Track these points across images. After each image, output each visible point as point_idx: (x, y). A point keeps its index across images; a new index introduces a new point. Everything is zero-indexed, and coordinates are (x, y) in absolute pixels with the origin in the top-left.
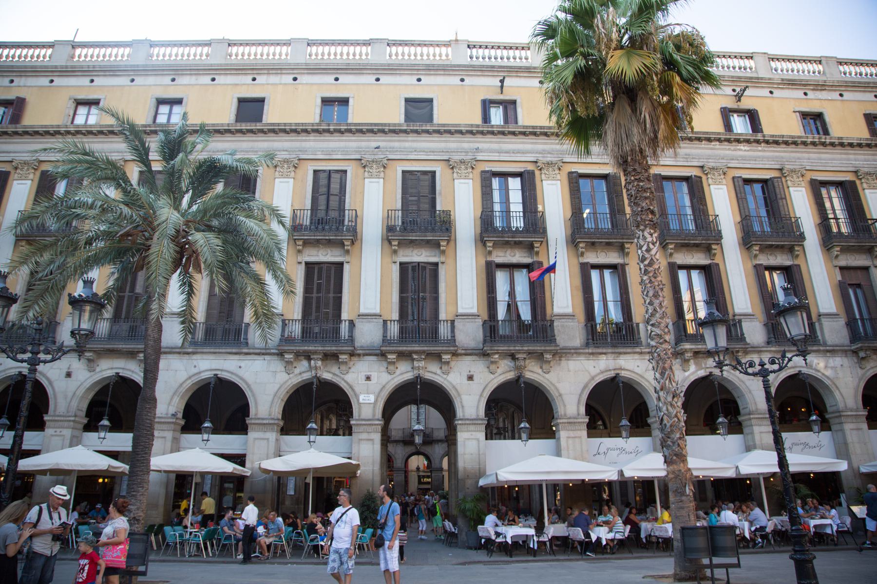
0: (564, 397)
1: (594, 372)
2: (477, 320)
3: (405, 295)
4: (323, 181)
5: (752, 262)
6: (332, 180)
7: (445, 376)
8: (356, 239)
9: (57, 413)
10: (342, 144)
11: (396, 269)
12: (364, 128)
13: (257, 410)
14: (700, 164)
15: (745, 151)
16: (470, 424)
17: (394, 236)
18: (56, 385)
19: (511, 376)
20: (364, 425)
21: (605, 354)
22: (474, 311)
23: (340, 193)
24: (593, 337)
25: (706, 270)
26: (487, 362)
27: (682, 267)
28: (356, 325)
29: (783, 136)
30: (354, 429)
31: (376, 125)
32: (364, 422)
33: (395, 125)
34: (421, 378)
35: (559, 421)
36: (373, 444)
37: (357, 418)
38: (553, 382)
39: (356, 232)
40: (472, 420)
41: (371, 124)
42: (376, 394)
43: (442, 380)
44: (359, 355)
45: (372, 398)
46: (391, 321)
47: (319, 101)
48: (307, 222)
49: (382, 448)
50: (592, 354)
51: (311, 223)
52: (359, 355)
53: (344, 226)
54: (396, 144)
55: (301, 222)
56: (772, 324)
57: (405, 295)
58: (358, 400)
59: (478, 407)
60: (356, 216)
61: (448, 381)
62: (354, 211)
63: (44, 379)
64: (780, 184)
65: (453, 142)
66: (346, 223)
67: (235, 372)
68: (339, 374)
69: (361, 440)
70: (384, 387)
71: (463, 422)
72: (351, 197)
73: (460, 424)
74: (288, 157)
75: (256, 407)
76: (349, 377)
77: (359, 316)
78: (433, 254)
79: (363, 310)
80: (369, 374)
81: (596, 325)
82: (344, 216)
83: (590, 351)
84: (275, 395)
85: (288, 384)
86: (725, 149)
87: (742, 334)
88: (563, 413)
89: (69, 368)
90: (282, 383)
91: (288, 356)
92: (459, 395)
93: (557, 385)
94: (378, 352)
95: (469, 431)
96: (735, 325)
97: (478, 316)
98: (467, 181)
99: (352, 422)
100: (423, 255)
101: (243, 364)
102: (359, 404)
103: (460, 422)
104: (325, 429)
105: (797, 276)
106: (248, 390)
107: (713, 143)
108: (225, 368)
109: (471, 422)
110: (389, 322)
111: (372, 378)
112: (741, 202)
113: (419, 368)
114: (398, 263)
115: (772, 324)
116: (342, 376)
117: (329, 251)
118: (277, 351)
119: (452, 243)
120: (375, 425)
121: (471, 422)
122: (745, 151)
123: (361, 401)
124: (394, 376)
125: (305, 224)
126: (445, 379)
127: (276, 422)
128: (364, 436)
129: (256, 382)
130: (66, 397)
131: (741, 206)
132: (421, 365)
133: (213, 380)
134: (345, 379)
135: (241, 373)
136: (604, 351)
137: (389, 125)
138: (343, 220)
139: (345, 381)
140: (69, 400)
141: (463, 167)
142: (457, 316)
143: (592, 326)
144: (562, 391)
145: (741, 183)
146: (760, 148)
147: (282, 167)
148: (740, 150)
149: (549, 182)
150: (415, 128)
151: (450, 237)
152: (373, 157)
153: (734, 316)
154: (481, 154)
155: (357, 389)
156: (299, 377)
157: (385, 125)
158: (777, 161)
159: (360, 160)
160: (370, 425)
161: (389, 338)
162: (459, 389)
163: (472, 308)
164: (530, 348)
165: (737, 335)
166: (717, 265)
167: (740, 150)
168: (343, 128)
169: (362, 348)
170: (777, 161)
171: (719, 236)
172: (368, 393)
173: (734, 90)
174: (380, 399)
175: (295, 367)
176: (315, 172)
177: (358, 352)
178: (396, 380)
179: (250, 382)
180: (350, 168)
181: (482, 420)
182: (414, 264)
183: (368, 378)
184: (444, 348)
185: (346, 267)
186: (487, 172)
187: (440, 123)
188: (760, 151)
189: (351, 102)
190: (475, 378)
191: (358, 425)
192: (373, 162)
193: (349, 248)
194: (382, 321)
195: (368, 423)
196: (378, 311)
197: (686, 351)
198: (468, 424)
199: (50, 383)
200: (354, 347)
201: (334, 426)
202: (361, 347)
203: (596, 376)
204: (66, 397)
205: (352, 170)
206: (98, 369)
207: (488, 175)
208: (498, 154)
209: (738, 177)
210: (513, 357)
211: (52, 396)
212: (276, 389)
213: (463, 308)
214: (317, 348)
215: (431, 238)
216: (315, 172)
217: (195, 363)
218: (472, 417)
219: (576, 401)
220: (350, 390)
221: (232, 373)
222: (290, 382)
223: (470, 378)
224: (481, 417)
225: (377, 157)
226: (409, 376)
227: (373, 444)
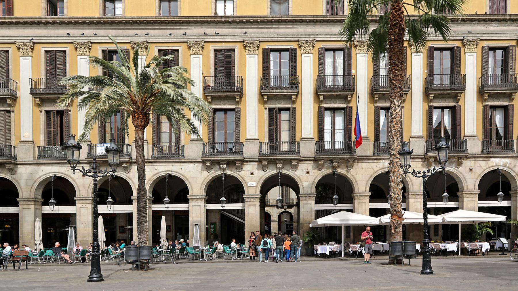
0: (358, 183)
1: (376, 169)
3: (272, 127)
5: (482, 103)
7: (294, 172)
8: (242, 95)
9: (81, 196)
10: (231, 31)
11: (267, 112)
13: (193, 192)
14: (461, 38)
16: (307, 196)
18: (77, 181)
19: (330, 171)
21: (383, 159)
24: (377, 150)
26: (317, 164)
28: (245, 145)
30: (245, 200)
34: (281, 173)
35: (354, 195)
36: (256, 207)
38: (353, 175)
39: (242, 90)
40: (308, 194)
42: (257, 182)
43: (292, 174)
45: (254, 184)
46: (264, 143)
48: (212, 84)
49: (261, 210)
50: (376, 159)
51: (215, 85)
53: (235, 87)
54: (265, 30)
55: (209, 84)
56: (487, 141)
57: (272, 127)
58: (247, 185)
59: (311, 188)
60: (242, 80)
61: (295, 174)
62: (240, 77)
63: (69, 178)
66: (236, 85)
67: (179, 172)
71: (303, 196)
72: (238, 67)
73: (302, 197)
75: (192, 190)
76: (242, 173)
77: (246, 140)
78: (288, 103)
80: (252, 171)
81: (380, 143)
82: (235, 79)
83: (375, 157)
84: (202, 184)
85: (209, 177)
87: (466, 148)
88: (357, 190)
90: (205, 177)
91: (208, 164)
92: (301, 182)
93: (355, 176)
94: (258, 159)
95: (306, 200)
96: (463, 143)
98: (309, 55)
99: (244, 196)
100: (282, 103)
101: (183, 167)
102: (248, 187)
103: (301, 195)
104: (230, 200)
105: (510, 112)
106: (187, 181)
107: (473, 23)
108: (173, 170)
109: (307, 195)
110: (263, 143)
111: (254, 174)
113: (280, 168)
114: (268, 109)
115: (487, 141)
117: (227, 102)
118: (201, 160)
119: (299, 96)
121: (307, 195)
123: (249, 185)
124: (266, 172)
125: (211, 85)
126: (294, 174)
127: (204, 197)
129: (191, 177)
130: (84, 187)
132: (281, 166)
133: (167, 176)
135: (182, 172)
136: (383, 157)
138: (234, 83)
139: (240, 176)
140: (87, 188)
141: (307, 45)
142: (301, 139)
143: (377, 144)
144: (357, 179)
149: (361, 55)
151: (298, 92)
152: (251, 40)
153: (464, 137)
155: (246, 179)
156: (215, 174)
159: (243, 42)
161: (263, 152)
162: (302, 180)
164: (341, 156)
165: (463, 148)
166: (460, 106)
174: (259, 184)
175: (212, 169)
176: (216, 51)
177: (246, 160)
178: (267, 174)
179: (188, 177)
180: (236, 47)
181: (313, 194)
182: (276, 109)
183: (252, 174)
184: (293, 157)
190: (310, 173)
192: (251, 43)
193: (239, 100)
194: (259, 142)
195: (253, 197)
196: (256, 137)
197: (430, 157)
198: (305, 197)
199: (74, 180)
200: (244, 157)
201: (235, 198)
204: (84, 187)
205: (238, 48)
210: (332, 161)
211: (77, 187)
212: (202, 180)
214: (223, 158)
215: (287, 93)
216: (216, 51)
217: (156, 167)
218: (308, 193)
219: (365, 184)
220: (242, 180)
221: (177, 173)
222: (209, 177)
223: (308, 173)
224: (312, 193)
226: (274, 172)
227: (256, 207)
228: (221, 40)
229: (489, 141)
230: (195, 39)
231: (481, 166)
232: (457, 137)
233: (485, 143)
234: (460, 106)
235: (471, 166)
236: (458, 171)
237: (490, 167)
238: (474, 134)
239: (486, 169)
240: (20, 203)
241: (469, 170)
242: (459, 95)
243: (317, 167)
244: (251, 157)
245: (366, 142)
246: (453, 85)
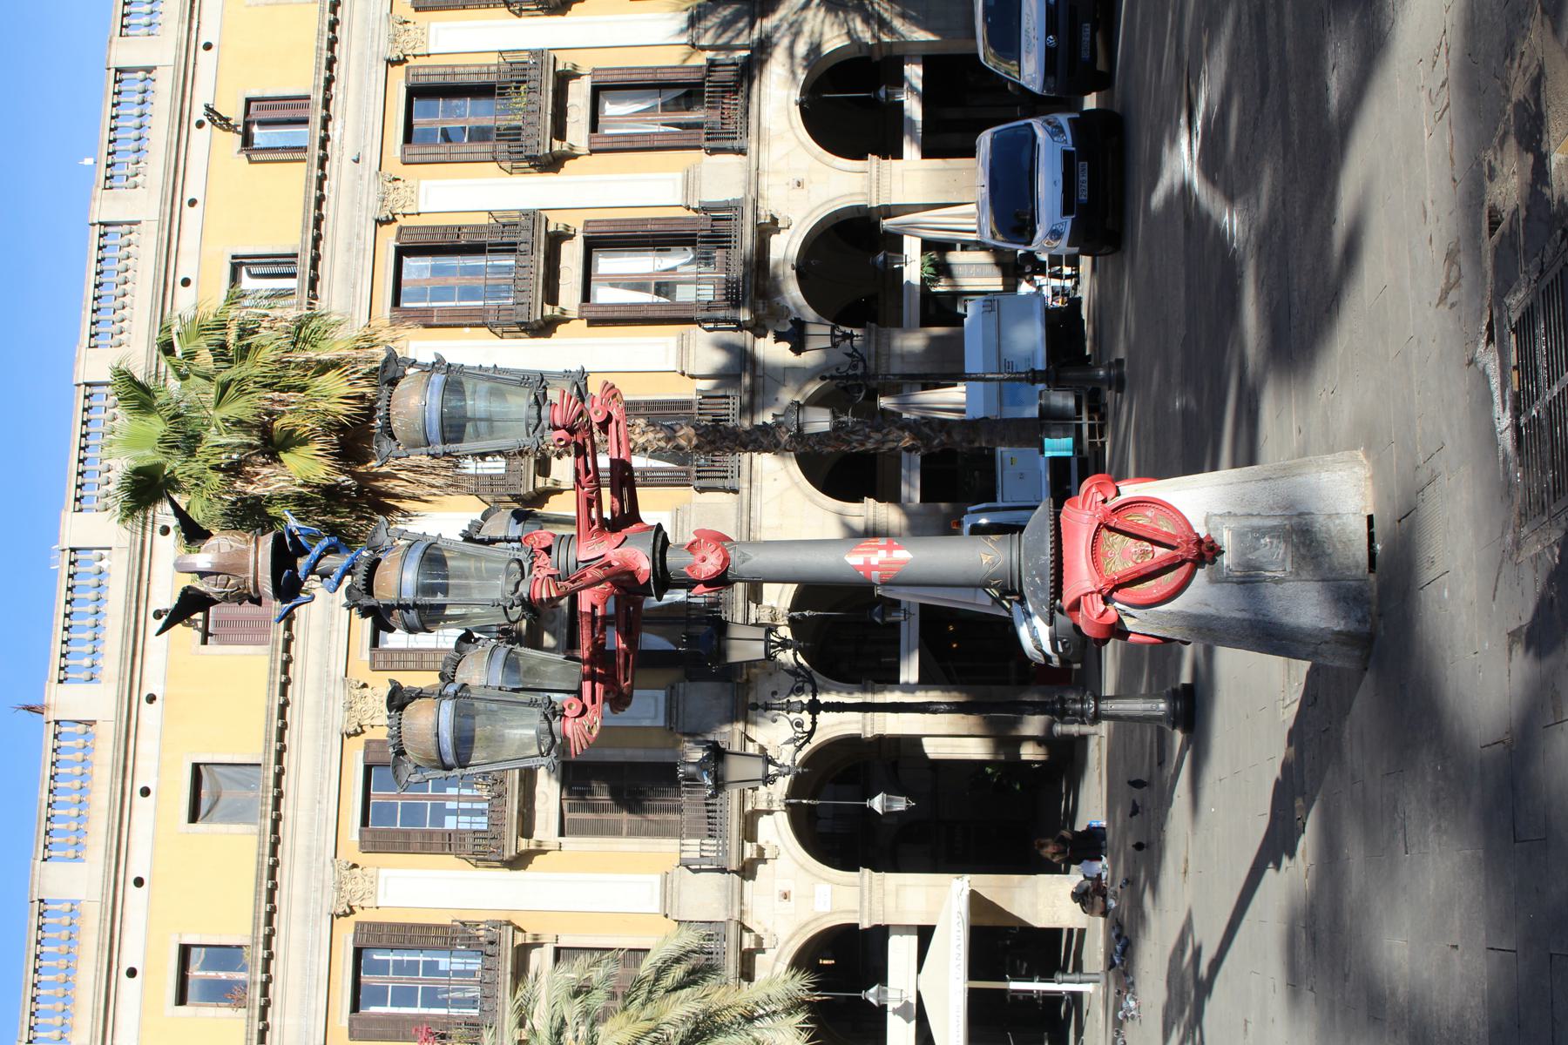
2: (681, 691)
11: (569, 842)
15: (343, 127)
17: (510, 846)
20: (870, 902)
22: (661, 694)
25: (594, 244)
27: (586, 295)
29: (319, 49)
31: (258, 884)
32: (866, 904)
33: (261, 845)
37: (858, 915)
41: (257, 893)
44: (742, 912)
45: (823, 889)
46: (682, 851)
52: (742, 912)
64: (421, 71)
65: (301, 723)
68: (777, 950)
69: (897, 907)
70: (802, 866)
79: (655, 907)
80: (777, 895)
86: (339, 168)
97: (673, 688)
102: (831, 914)
110: (684, 855)
111: (786, 889)
112: (456, 157)
116: (780, 944)
120: (871, 882)
122: (343, 127)
123: (828, 910)
128: (890, 902)
131: (464, 157)
134: (785, 938)
137: (260, 855)
141: (359, 706)
145: (413, 149)
146: (340, 97)
148: (342, 136)
150: (270, 801)
154: (332, 667)
155: (805, 917)
157: (260, 864)
158: (371, 67)
160: (870, 891)
163: (656, 700)
166: (587, 223)
167: (342, 136)
168: (261, 953)
169: (728, 906)
170: (371, 67)
171: (533, 216)
172: (814, 896)
173: (200, 124)
186: (373, 657)
187: (261, 750)
188: (345, 98)
189: (186, 941)
191: (870, 915)
196: (656, 879)
202: (727, 909)
203: (791, 477)
207: (381, 657)
208: (335, 635)
209: (403, 152)
213: (656, 717)
220: (807, 929)
225: (330, 883)
226: (782, 819)
229: (708, 134)
231: (787, 154)
232: (687, 229)
233: (712, 144)
234: (587, 223)
235: (788, 184)
236: (801, 223)
237: (792, 128)
238: (679, 177)
239: (797, 137)
241: (798, 191)
242: (551, 229)
243: (770, 674)
244: (726, 897)
245: (693, 515)
246: (522, 247)
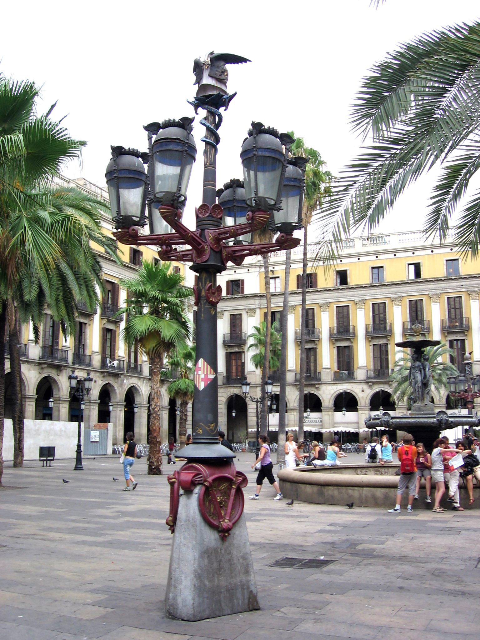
4: (452, 303)
6: (456, 302)
9: (362, 405)
12: (468, 276)
18: (359, 395)
23: (460, 307)
47: (445, 262)
74: (435, 293)
89: (362, 388)
147: (433, 298)
176: (448, 298)
185: (466, 342)
206: (374, 388)
216: (448, 298)
228: (452, 291)
230: (433, 292)
240: (323, 411)
